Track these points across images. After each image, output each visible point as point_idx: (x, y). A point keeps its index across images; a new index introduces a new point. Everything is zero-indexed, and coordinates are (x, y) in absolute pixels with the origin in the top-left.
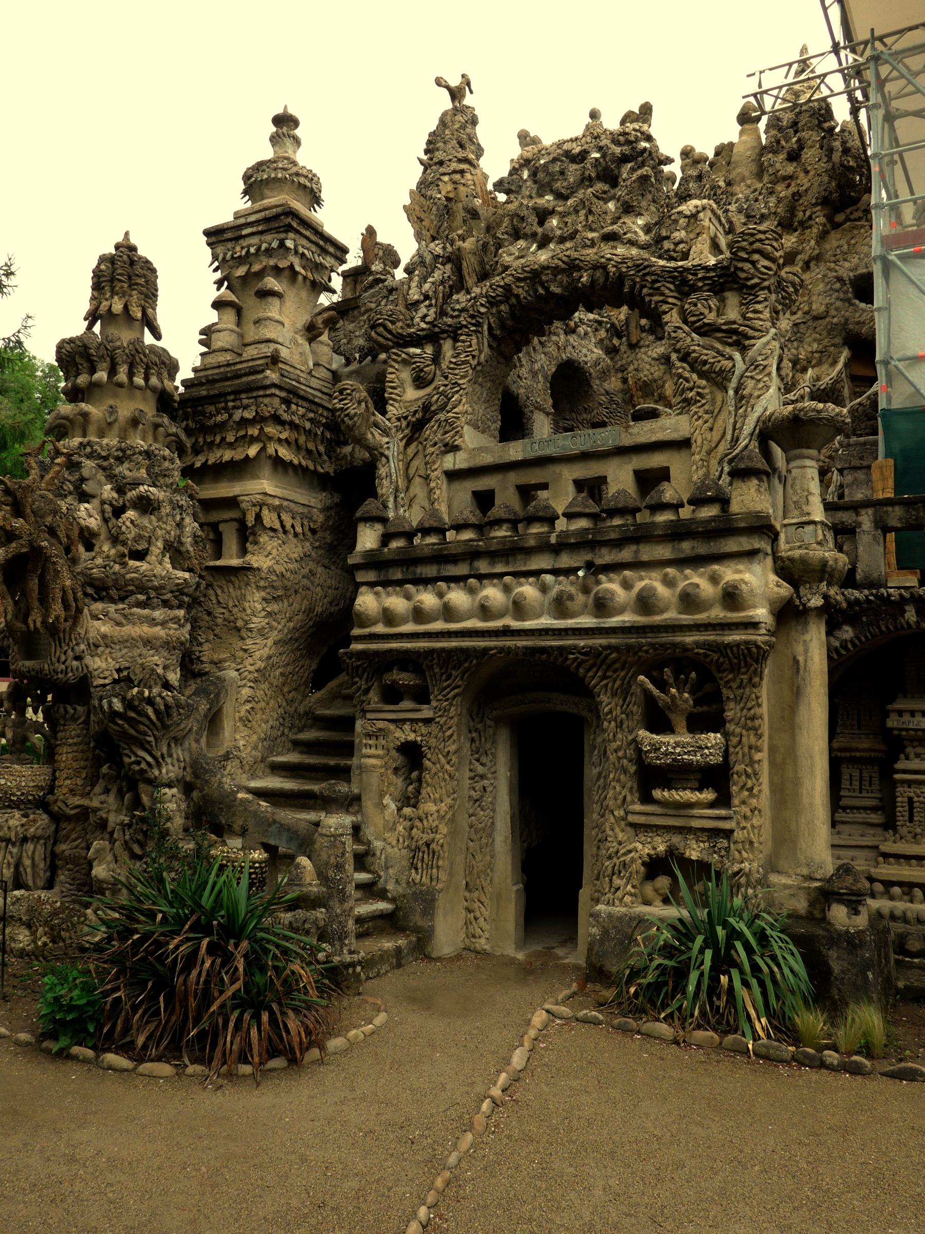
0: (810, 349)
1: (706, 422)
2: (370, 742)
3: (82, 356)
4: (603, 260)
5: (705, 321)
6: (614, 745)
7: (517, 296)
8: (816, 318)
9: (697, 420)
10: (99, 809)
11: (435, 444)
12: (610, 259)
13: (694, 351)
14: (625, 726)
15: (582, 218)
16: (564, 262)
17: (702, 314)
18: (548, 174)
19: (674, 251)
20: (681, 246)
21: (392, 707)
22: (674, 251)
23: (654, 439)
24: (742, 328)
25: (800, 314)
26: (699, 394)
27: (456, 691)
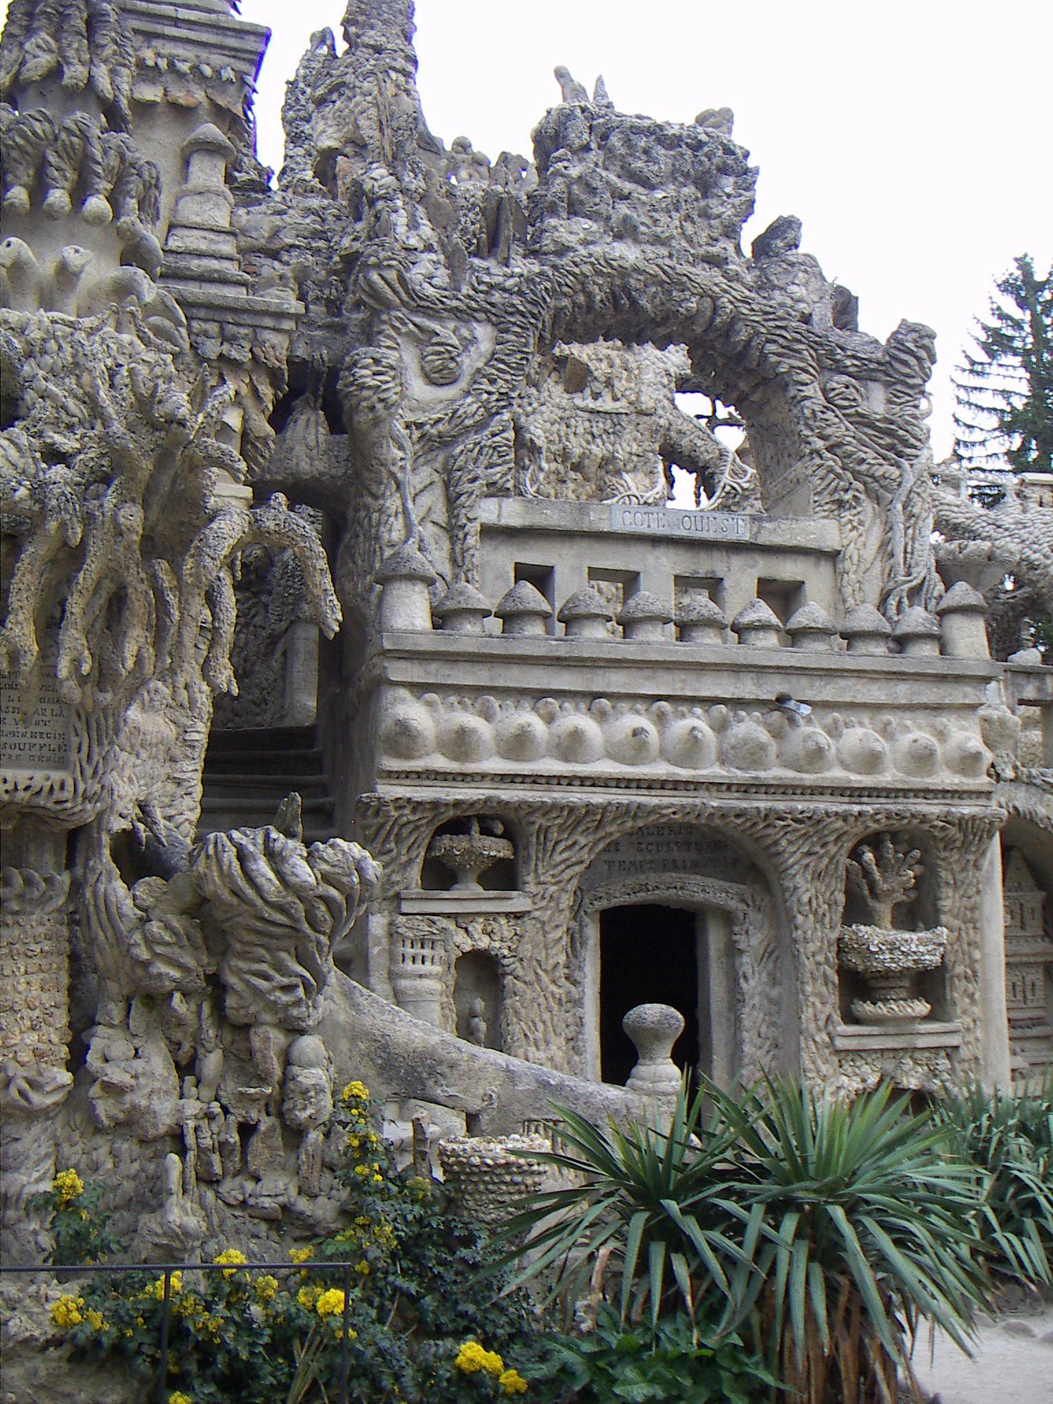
0: (628, 449)
1: (861, 535)
2: (427, 952)
3: (67, 152)
4: (716, 289)
5: (859, 410)
6: (812, 947)
7: (589, 296)
8: (642, 413)
9: (851, 531)
10: (132, 1089)
11: (474, 480)
12: (726, 292)
13: (849, 444)
14: (827, 919)
15: (677, 223)
16: (665, 272)
17: (855, 400)
18: (628, 142)
19: (792, 307)
20: (802, 305)
21: (445, 894)
22: (792, 307)
23: (793, 543)
24: (901, 432)
25: (624, 402)
26: (855, 496)
27: (577, 869)
